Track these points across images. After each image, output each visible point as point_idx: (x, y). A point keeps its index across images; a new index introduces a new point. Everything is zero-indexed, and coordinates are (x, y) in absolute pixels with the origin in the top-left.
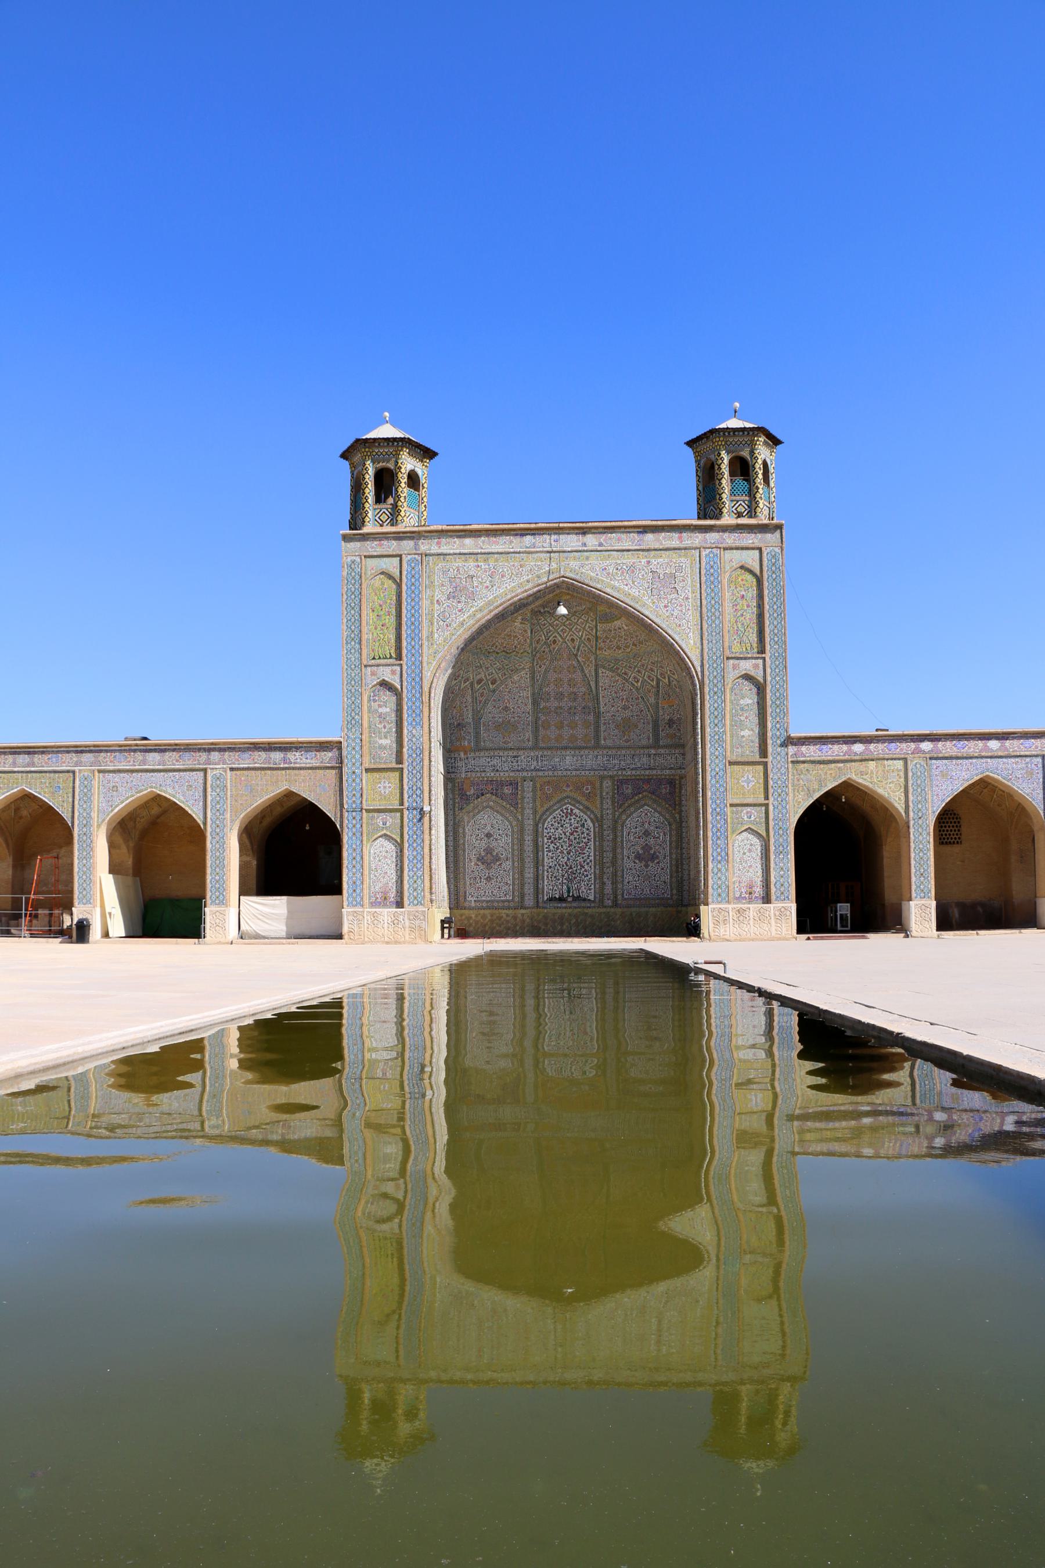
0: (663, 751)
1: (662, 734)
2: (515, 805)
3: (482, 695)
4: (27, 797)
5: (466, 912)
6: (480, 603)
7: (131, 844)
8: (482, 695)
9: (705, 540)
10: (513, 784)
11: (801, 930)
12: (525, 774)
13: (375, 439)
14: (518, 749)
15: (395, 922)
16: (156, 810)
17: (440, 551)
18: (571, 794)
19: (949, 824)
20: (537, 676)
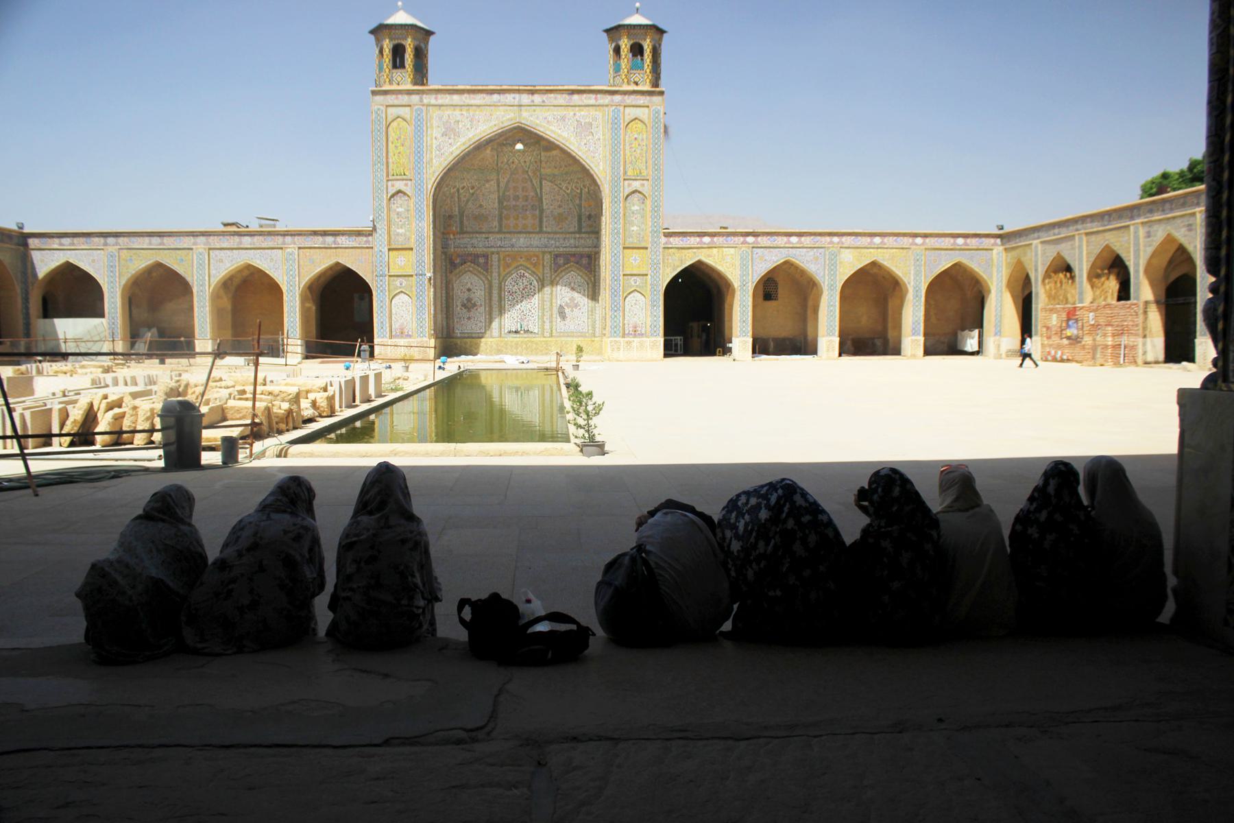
2: (487, 270)
4: (159, 265)
6: (462, 140)
10: (486, 256)
11: (666, 355)
16: (246, 273)
19: (768, 289)
20: (502, 185)
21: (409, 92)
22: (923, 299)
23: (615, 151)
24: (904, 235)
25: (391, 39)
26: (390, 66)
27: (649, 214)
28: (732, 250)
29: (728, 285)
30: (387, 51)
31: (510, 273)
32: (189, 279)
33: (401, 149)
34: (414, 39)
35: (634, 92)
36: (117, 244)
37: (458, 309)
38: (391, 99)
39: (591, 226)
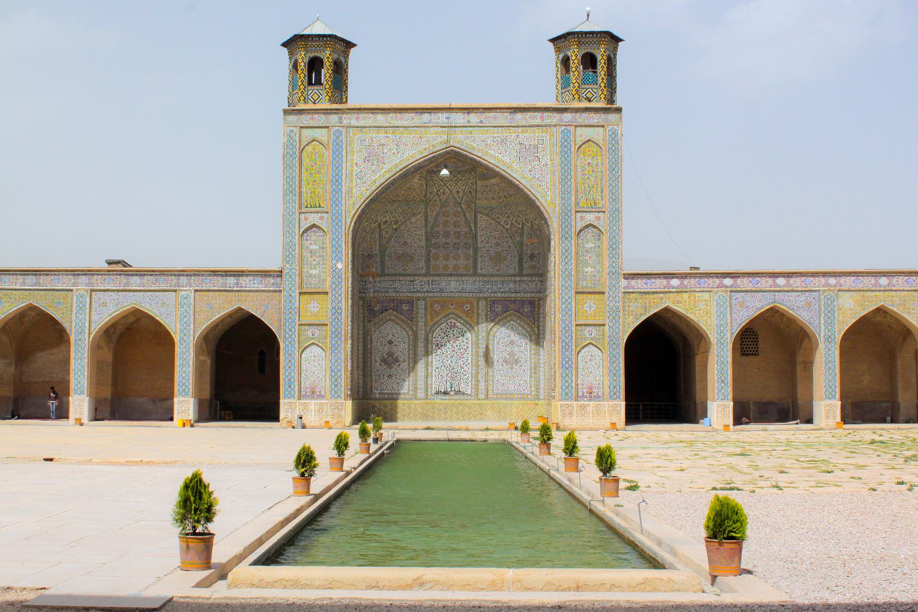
0: (525, 278)
1: (525, 266)
2: (411, 320)
3: (387, 232)
4: (32, 308)
5: (372, 402)
6: (388, 166)
7: (112, 345)
8: (387, 232)
9: (562, 120)
10: (410, 302)
12: (419, 295)
13: (309, 36)
14: (415, 275)
15: (320, 411)
16: (131, 319)
17: (358, 125)
18: (455, 312)
20: (430, 219)
21: (326, 112)
23: (565, 177)
25: (307, 51)
26: (306, 83)
27: (606, 252)
29: (701, 336)
30: (302, 66)
31: (438, 323)
32: (66, 325)
35: (587, 110)
37: (377, 365)
38: (305, 119)
39: (533, 267)
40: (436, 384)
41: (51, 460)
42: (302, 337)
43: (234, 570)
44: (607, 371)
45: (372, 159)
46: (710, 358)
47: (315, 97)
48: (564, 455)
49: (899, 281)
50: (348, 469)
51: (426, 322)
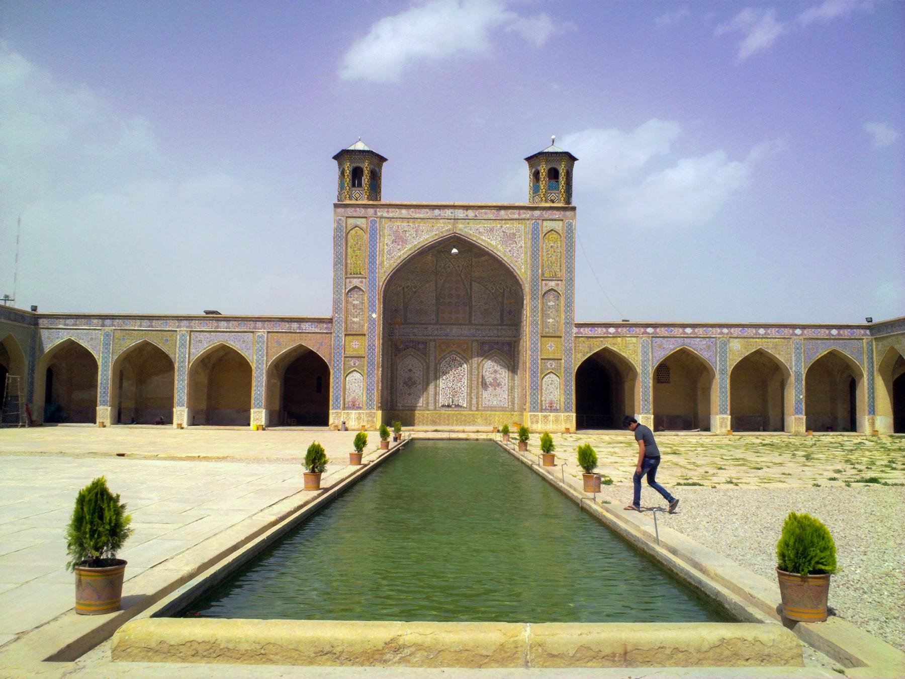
1: (505, 318)
2: (425, 354)
4: (147, 344)
6: (409, 246)
9: (533, 215)
10: (425, 343)
15: (359, 418)
16: (222, 353)
19: (662, 372)
21: (365, 206)
22: (804, 382)
23: (535, 253)
24: (785, 326)
25: (351, 163)
26: (350, 185)
27: (563, 309)
28: (634, 340)
31: (444, 358)
32: (172, 356)
33: (358, 252)
34: (370, 163)
36: (113, 325)
38: (350, 211)
40: (442, 400)
41: (123, 455)
42: (347, 367)
43: (124, 627)
44: (563, 392)
45: (399, 242)
46: (637, 384)
47: (357, 195)
48: (542, 452)
49: (773, 332)
50: (366, 463)
51: (435, 357)
